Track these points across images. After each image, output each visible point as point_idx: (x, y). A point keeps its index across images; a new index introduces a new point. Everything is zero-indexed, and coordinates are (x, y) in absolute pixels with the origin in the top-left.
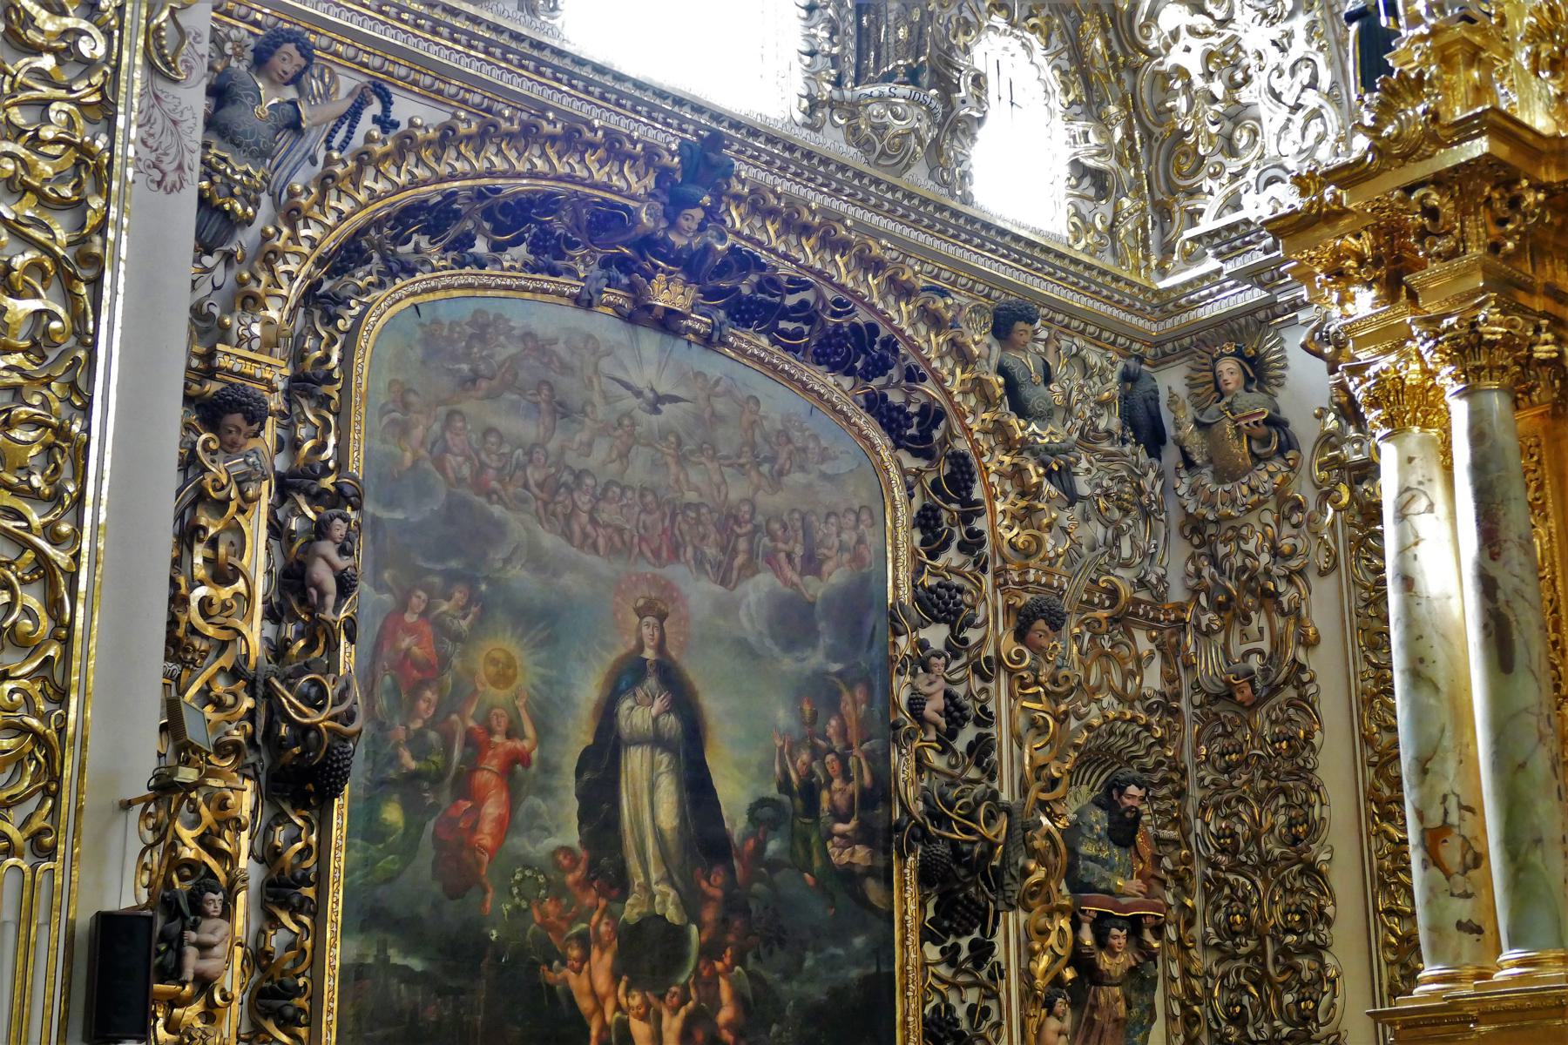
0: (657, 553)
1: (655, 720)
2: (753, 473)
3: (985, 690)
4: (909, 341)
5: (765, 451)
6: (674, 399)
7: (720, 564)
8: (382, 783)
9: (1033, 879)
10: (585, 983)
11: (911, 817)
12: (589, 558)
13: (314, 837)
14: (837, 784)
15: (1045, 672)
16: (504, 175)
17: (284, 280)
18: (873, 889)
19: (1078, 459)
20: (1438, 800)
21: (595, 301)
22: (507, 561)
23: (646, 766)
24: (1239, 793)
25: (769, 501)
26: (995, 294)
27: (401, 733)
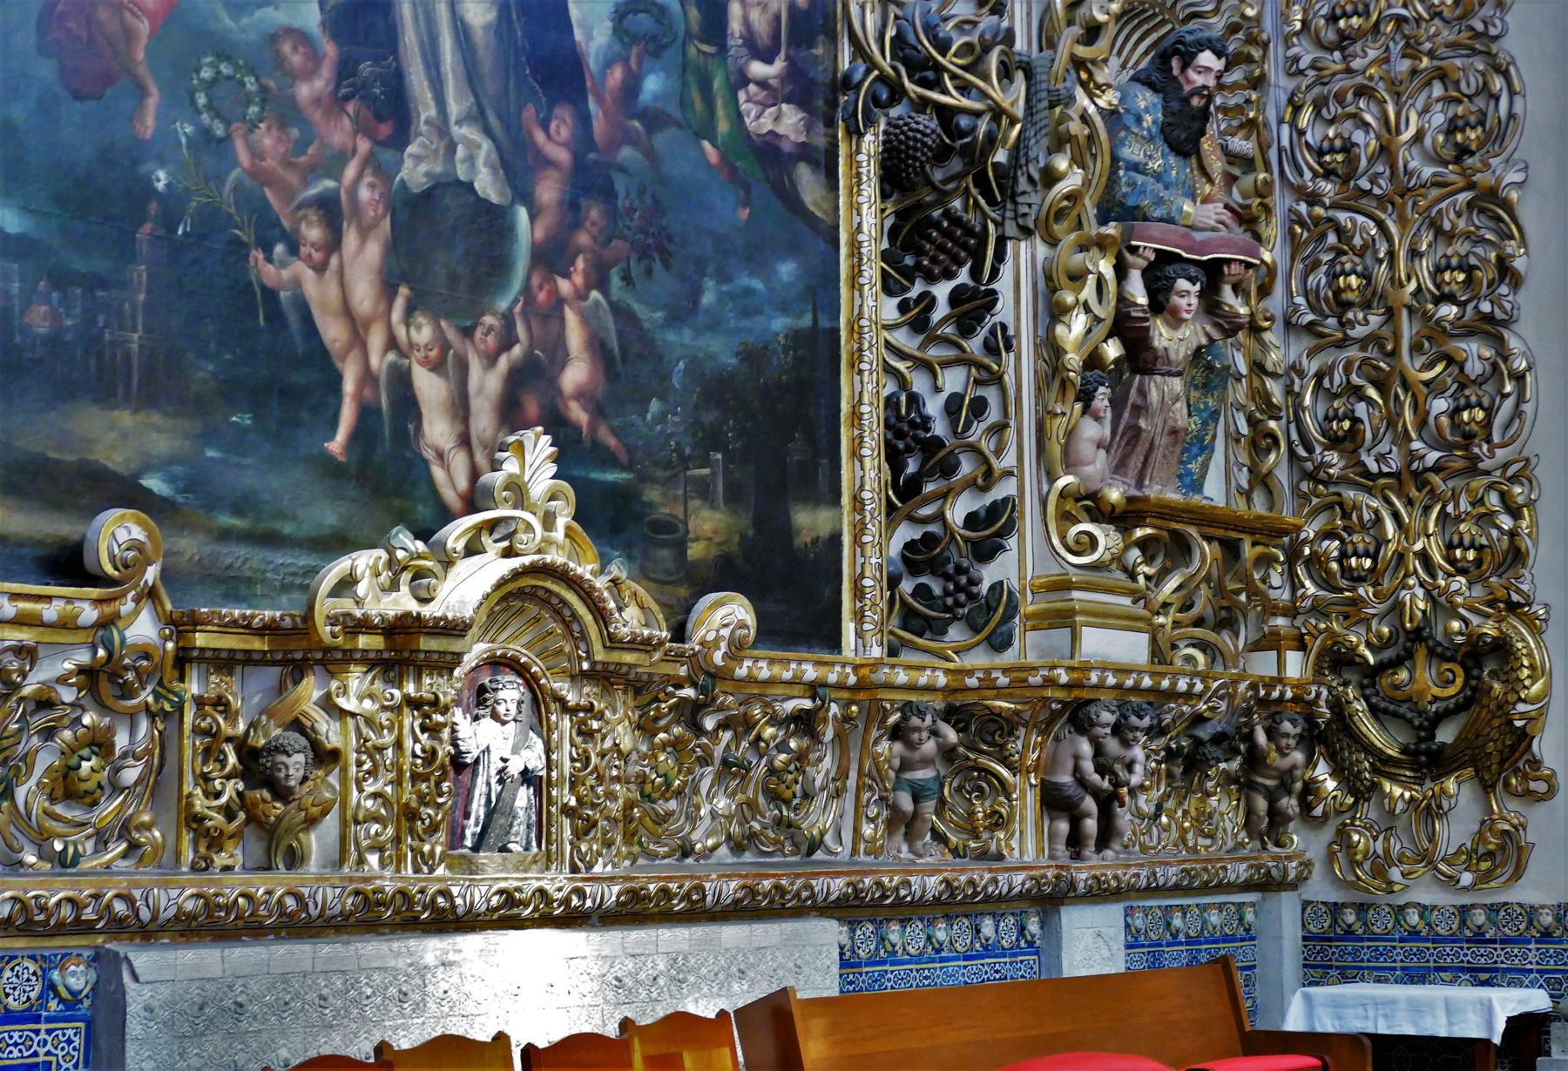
9: (1063, 187)
10: (333, 291)
11: (872, 65)
18: (808, 183)
24: (1359, 79)
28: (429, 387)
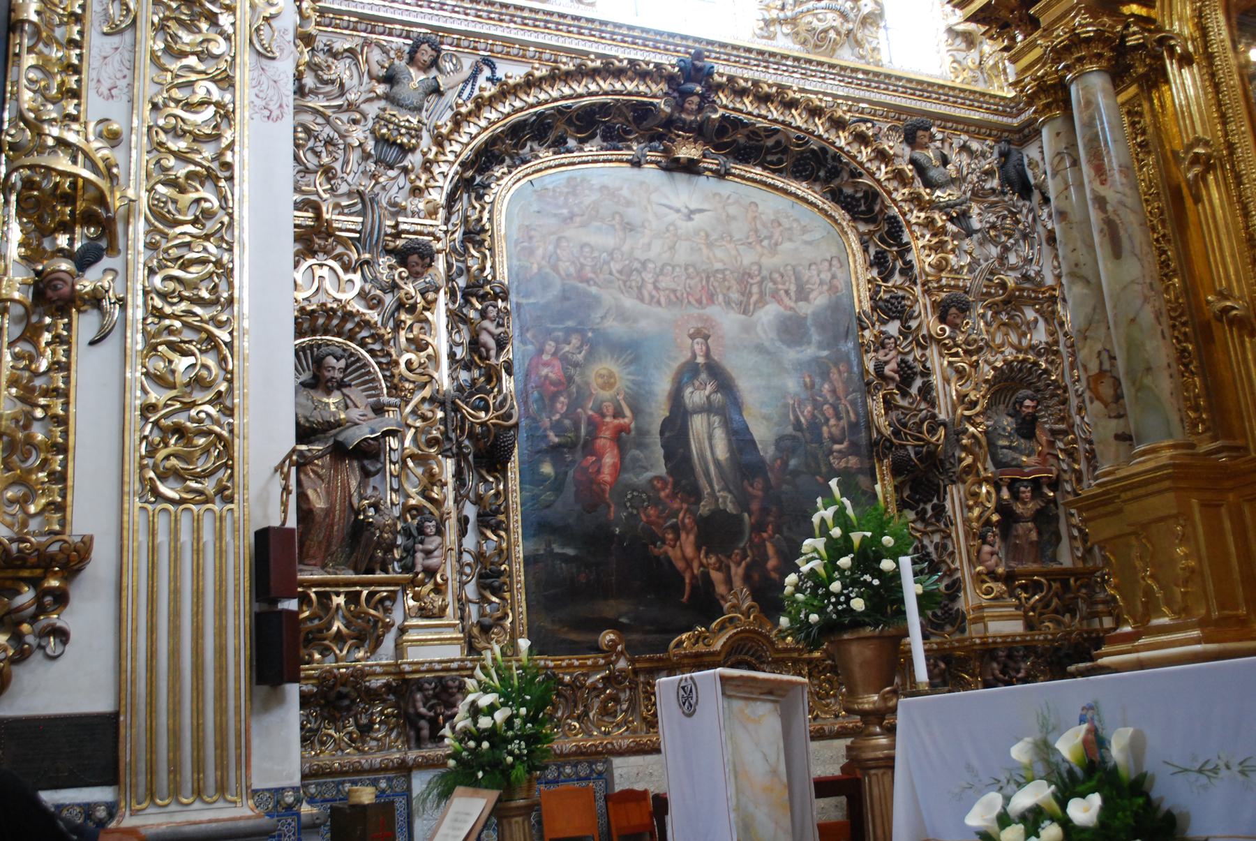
0: (699, 302)
1: (708, 397)
2: (758, 247)
3: (923, 355)
4: (848, 153)
5: (764, 233)
6: (701, 211)
7: (741, 303)
8: (539, 452)
9: (964, 463)
10: (679, 553)
12: (655, 309)
13: (501, 487)
14: (832, 422)
15: (960, 338)
16: (570, 97)
17: (440, 178)
19: (970, 208)
20: (1095, 356)
21: (643, 161)
22: (603, 318)
23: (705, 424)
25: (768, 262)
26: (903, 117)
27: (547, 423)
28: (716, 576)
